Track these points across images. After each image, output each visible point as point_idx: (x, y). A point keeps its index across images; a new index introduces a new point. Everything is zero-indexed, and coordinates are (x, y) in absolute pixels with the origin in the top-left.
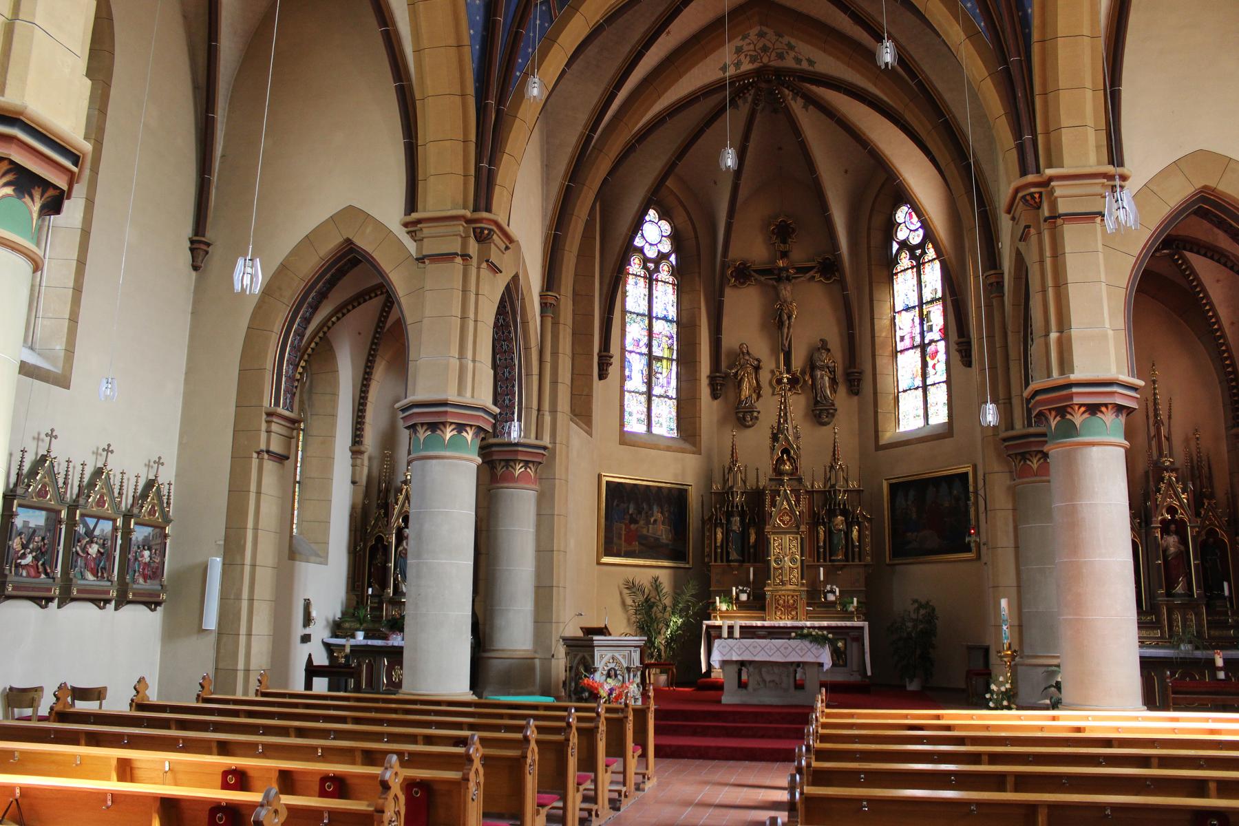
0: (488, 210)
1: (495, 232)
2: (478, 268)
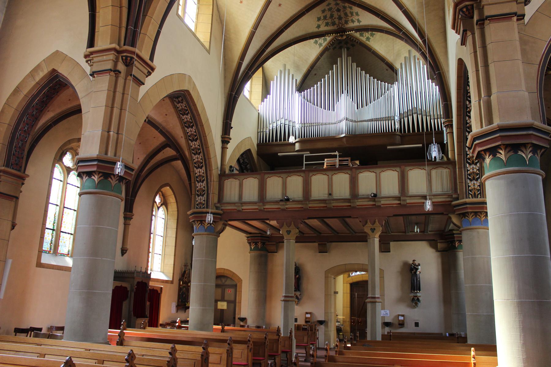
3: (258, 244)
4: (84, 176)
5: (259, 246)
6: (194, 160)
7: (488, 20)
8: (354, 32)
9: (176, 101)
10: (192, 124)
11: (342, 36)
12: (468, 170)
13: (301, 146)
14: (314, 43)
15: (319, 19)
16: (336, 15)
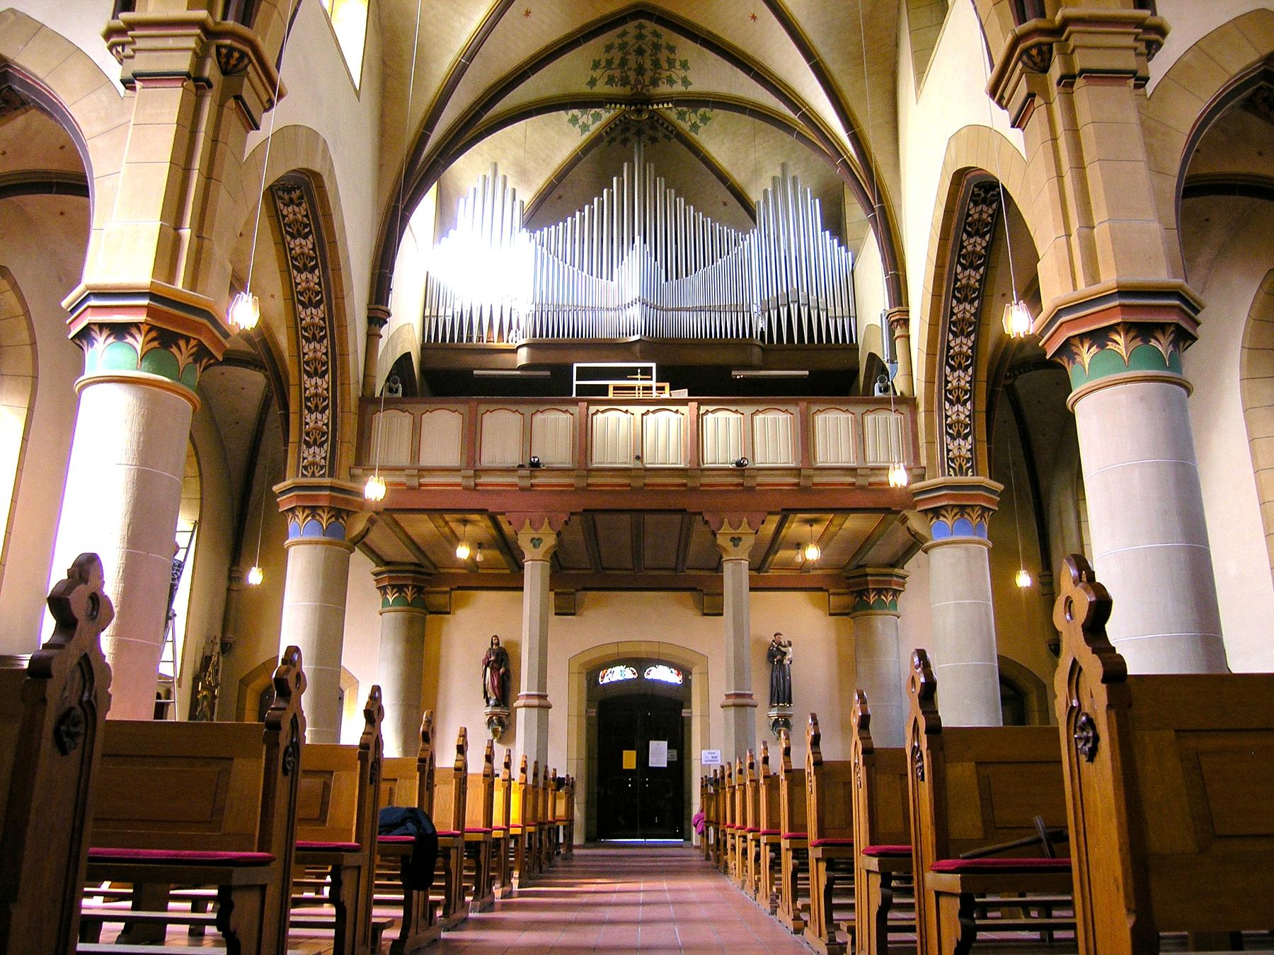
1: (250, 61)
2: (221, 106)
3: (406, 590)
4: (101, 334)
5: (406, 594)
6: (305, 354)
7: (1084, 77)
8: (670, 105)
9: (280, 198)
10: (313, 263)
11: (639, 112)
12: (947, 417)
13: (531, 356)
14: (570, 121)
15: (596, 65)
16: (632, 61)
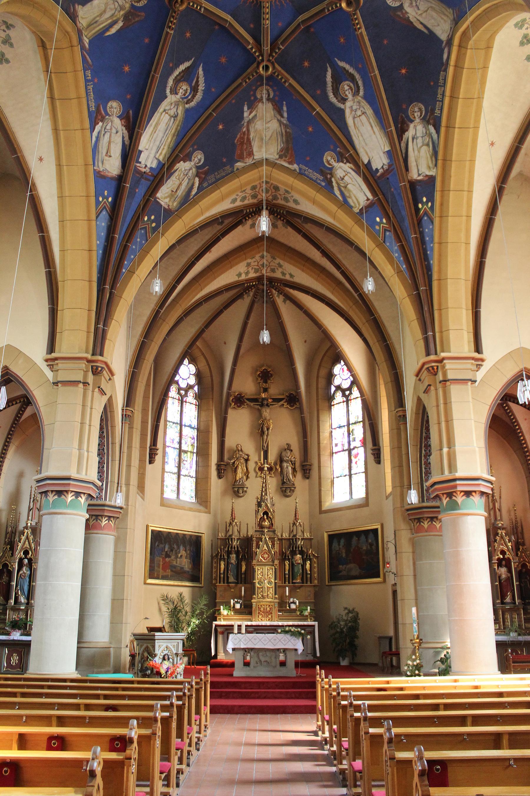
0: (101, 354)
1: (104, 369)
2: (93, 391)
